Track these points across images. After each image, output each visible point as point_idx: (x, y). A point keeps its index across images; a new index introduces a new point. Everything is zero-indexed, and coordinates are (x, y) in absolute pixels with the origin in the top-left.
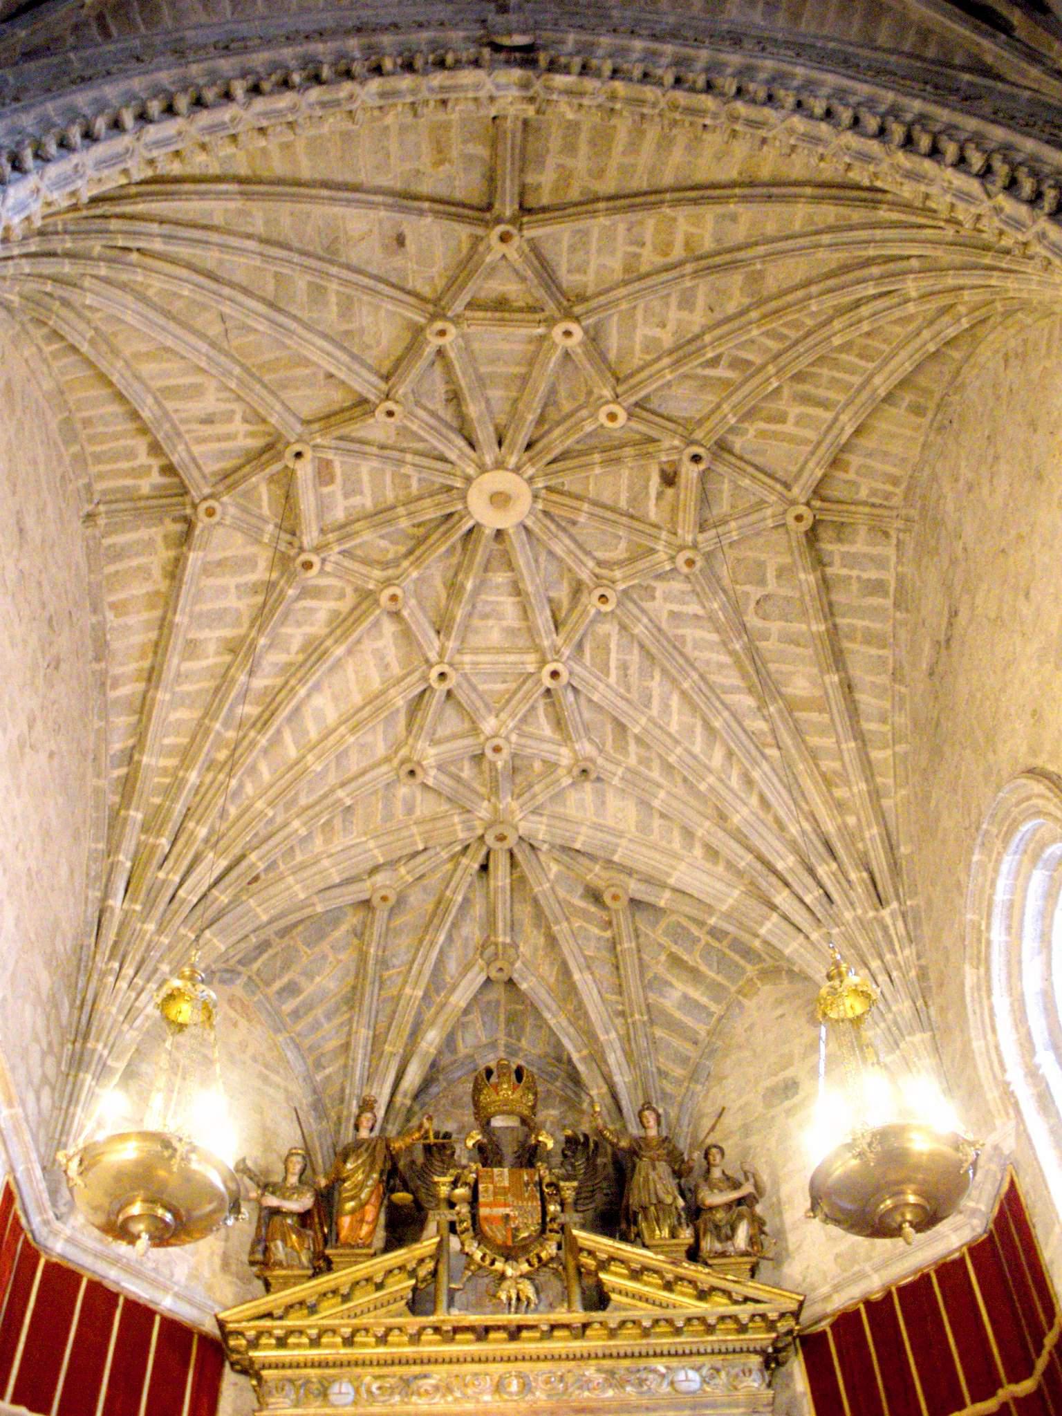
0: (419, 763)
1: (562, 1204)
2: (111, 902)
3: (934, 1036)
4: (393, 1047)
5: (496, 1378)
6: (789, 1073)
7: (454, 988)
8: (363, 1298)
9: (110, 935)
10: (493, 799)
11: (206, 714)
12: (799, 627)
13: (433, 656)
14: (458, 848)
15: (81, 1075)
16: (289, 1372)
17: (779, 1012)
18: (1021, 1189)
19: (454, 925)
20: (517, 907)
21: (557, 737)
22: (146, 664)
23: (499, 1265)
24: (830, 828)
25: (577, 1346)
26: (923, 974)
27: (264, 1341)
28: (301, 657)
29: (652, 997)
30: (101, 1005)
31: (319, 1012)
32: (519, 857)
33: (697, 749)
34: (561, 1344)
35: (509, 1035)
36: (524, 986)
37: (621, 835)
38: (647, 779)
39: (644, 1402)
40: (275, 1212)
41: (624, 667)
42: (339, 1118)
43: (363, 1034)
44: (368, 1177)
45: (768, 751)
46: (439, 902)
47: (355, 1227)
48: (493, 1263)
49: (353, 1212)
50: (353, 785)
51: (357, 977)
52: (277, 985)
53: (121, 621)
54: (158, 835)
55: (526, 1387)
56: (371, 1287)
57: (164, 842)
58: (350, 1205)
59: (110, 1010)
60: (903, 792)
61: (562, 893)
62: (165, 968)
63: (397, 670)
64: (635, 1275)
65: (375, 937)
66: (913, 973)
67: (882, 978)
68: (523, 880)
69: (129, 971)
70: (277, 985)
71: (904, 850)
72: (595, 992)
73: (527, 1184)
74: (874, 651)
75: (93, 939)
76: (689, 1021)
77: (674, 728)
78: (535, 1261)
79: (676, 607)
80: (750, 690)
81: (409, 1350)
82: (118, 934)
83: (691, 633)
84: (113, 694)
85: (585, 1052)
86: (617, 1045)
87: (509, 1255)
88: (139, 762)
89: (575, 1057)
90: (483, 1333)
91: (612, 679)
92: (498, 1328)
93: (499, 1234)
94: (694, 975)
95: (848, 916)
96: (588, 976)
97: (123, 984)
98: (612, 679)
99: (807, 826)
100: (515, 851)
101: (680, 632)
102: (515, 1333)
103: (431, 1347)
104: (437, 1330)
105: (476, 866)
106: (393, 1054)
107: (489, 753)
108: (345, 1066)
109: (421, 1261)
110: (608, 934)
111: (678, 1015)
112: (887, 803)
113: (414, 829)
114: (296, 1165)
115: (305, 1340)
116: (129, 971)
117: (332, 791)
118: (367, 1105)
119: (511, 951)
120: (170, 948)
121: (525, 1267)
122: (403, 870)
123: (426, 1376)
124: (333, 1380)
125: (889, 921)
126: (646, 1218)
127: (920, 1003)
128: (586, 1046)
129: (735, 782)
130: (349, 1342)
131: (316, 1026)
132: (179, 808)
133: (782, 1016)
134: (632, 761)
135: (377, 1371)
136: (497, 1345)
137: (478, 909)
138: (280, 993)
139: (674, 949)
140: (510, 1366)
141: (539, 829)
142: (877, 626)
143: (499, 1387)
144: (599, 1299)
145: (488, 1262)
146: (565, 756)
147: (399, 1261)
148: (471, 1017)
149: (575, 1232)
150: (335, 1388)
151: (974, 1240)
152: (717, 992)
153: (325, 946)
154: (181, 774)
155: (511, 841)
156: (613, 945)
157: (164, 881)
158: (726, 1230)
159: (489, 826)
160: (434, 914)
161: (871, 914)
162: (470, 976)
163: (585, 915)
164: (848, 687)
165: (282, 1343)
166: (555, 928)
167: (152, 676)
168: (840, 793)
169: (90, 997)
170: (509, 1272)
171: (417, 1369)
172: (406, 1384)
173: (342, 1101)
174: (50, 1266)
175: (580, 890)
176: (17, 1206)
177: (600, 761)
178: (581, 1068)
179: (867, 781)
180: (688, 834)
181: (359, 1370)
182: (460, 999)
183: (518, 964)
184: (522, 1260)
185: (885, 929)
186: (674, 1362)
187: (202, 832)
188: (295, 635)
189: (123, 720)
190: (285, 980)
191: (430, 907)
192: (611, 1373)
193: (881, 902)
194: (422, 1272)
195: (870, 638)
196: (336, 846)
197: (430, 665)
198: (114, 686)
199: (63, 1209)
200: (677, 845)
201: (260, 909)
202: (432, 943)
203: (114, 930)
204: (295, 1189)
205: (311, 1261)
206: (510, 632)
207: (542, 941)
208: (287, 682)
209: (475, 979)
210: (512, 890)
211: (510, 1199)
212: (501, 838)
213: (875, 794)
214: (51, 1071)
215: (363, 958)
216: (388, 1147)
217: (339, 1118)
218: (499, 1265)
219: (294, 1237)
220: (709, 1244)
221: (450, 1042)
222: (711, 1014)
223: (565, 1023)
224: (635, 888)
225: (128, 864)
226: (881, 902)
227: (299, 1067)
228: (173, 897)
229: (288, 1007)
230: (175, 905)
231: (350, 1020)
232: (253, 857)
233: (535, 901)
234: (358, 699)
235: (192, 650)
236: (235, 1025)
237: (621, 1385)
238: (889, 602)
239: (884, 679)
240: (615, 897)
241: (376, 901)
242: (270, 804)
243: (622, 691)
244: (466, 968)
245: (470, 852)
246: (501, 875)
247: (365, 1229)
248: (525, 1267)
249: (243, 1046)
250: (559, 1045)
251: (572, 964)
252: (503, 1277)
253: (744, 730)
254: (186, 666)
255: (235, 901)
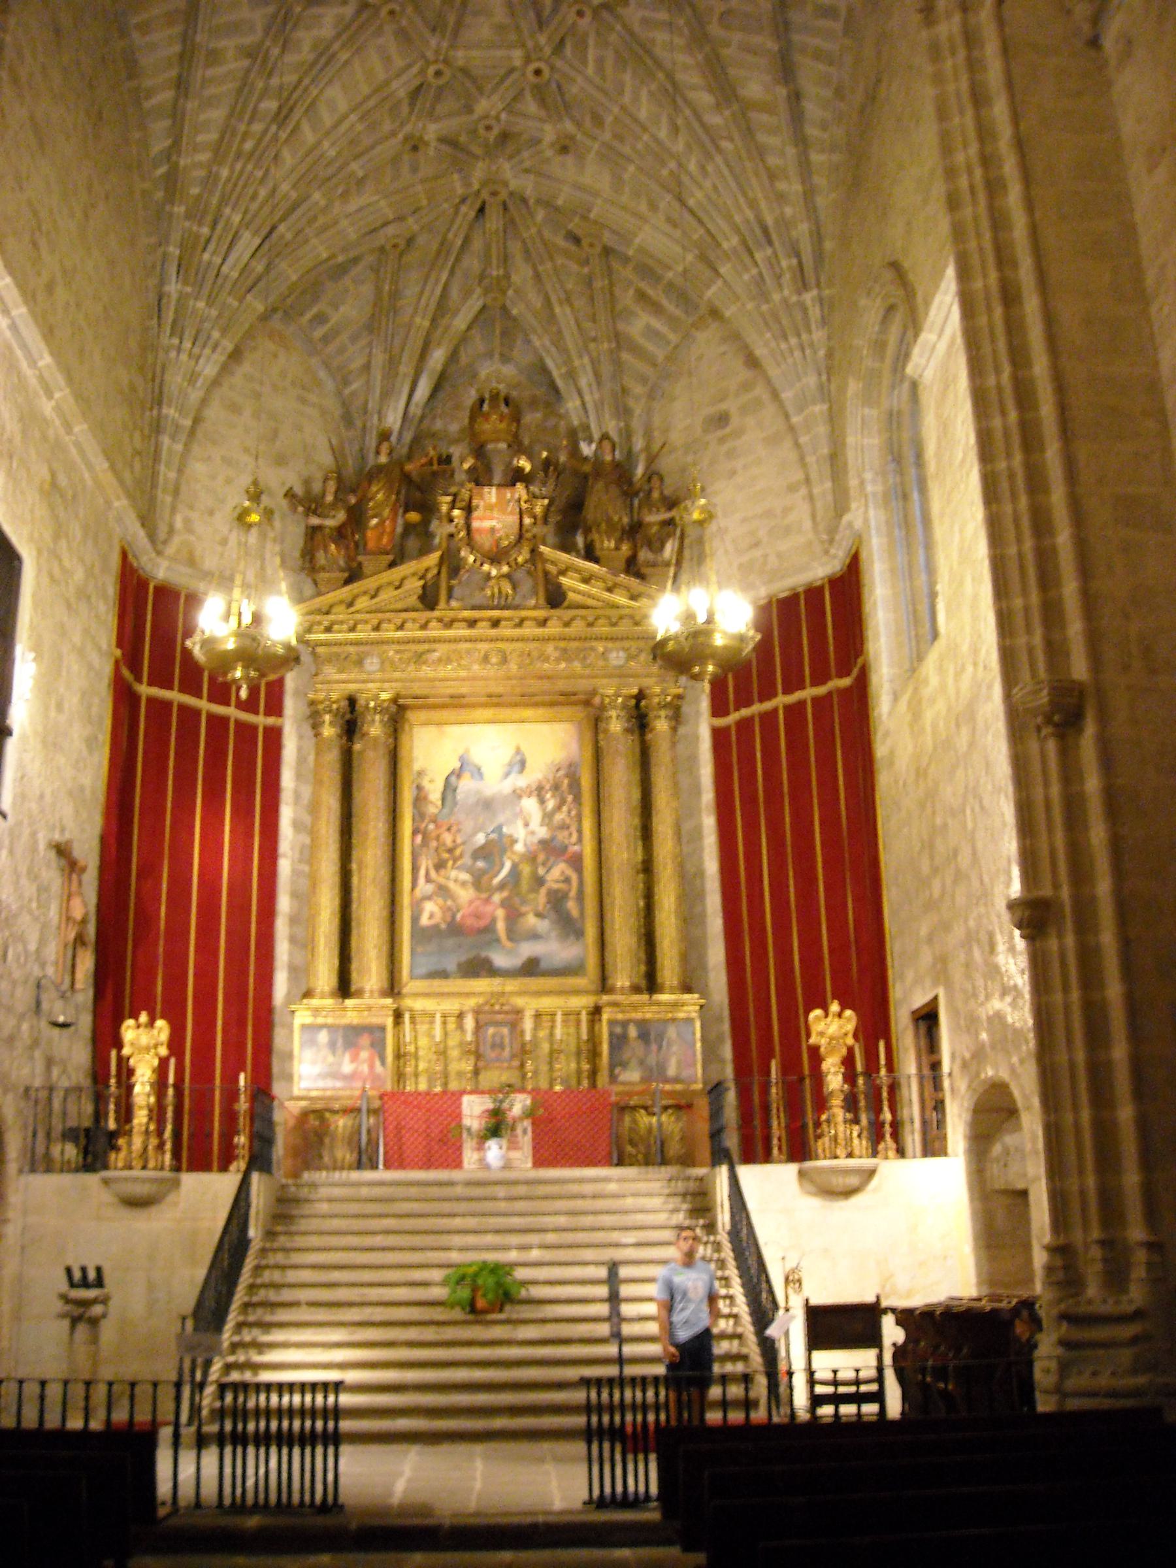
0: (421, 138)
1: (535, 517)
2: (167, 288)
3: (830, 408)
4: (406, 368)
5: (483, 653)
6: (723, 406)
7: (458, 311)
8: (386, 595)
9: (170, 315)
10: (487, 161)
11: (231, 115)
12: (756, 40)
13: (430, 55)
14: (457, 200)
15: (161, 438)
16: (335, 649)
17: (723, 348)
18: (864, 555)
19: (458, 260)
20: (509, 243)
21: (543, 113)
22: (174, 73)
23: (486, 567)
24: (769, 220)
25: (539, 631)
26: (830, 355)
27: (315, 628)
28: (311, 57)
29: (621, 326)
30: (167, 377)
31: (344, 337)
32: (511, 207)
33: (663, 134)
34: (529, 630)
35: (502, 345)
36: (515, 312)
37: (596, 194)
38: (620, 154)
39: (587, 672)
40: (318, 528)
41: (600, 61)
42: (364, 427)
43: (379, 358)
44: (387, 498)
45: (725, 144)
46: (442, 244)
47: (380, 538)
48: (482, 565)
49: (376, 526)
50: (365, 158)
51: (375, 305)
52: (309, 315)
53: (147, 39)
54: (200, 224)
55: (504, 660)
56: (391, 588)
57: (205, 231)
58: (374, 521)
59: (175, 380)
60: (834, 195)
61: (547, 234)
62: (216, 334)
63: (399, 63)
64: (586, 581)
65: (389, 276)
66: (822, 353)
67: (797, 354)
68: (512, 222)
69: (187, 345)
70: (309, 315)
71: (828, 245)
72: (572, 322)
73: (509, 501)
74: (821, 67)
75: (155, 321)
76: (650, 347)
77: (643, 114)
78: (513, 564)
79: (648, 14)
80: (710, 90)
81: (420, 634)
82: (176, 312)
83: (661, 37)
84: (147, 105)
85: (564, 370)
86: (589, 368)
87: (495, 560)
88: (177, 163)
89: (556, 374)
90: (472, 623)
91: (590, 70)
92: (482, 620)
93: (485, 541)
94: (657, 309)
95: (776, 297)
96: (568, 310)
97: (184, 357)
98: (590, 70)
99: (750, 215)
100: (508, 201)
101: (651, 35)
102: (496, 623)
103: (435, 631)
104: (440, 620)
105: (472, 214)
106: (405, 375)
107: (482, 131)
108: (368, 382)
109: (427, 570)
110: (586, 270)
111: (642, 341)
112: (820, 201)
113: (419, 188)
114: (332, 486)
115: (345, 627)
116: (187, 345)
117: (346, 164)
118: (385, 436)
119: (504, 283)
120: (219, 316)
121: (505, 569)
122: (410, 220)
123: (434, 651)
124: (367, 654)
125: (809, 303)
126: (599, 532)
127: (824, 378)
128: (565, 363)
129: (692, 167)
130: (377, 628)
131: (342, 350)
132: (215, 201)
133: (724, 353)
134: (607, 136)
135: (397, 647)
136: (483, 629)
137: (477, 244)
138: (311, 321)
139: (643, 285)
140: (492, 645)
141: (527, 185)
142: (826, 45)
143: (486, 659)
144: (555, 598)
145: (478, 563)
146: (549, 133)
147: (412, 570)
148: (473, 331)
149: (542, 548)
150: (368, 661)
151: (833, 574)
152: (673, 321)
153: (347, 281)
154: (215, 169)
155: (504, 195)
156: (589, 281)
157: (209, 263)
158: (657, 545)
159: (484, 184)
160: (439, 253)
161: (794, 299)
162: (469, 302)
163: (567, 254)
164: (796, 97)
165: (328, 630)
166: (541, 268)
167: (181, 85)
168: (781, 186)
169: (158, 369)
170: (494, 572)
171: (426, 646)
172: (419, 658)
173: (366, 412)
174: (156, 588)
175: (563, 232)
176: (130, 556)
177: (579, 137)
178: (560, 383)
179: (803, 182)
180: (653, 207)
181: (385, 647)
182: (460, 322)
183: (510, 292)
184: (504, 563)
185: (805, 310)
186: (610, 645)
187: (237, 219)
188: (306, 39)
189: (160, 126)
190: (315, 310)
191: (435, 246)
192: (565, 650)
193: (803, 285)
194: (430, 575)
195: (818, 55)
196: (352, 207)
197: (428, 63)
198: (148, 97)
199: (160, 547)
200: (643, 207)
201: (290, 272)
202: (437, 281)
203: (172, 308)
204: (333, 505)
205: (346, 563)
206: (500, 28)
207: (530, 273)
208: (300, 81)
209: (474, 304)
210: (505, 232)
211: (496, 514)
212: (494, 194)
213: (809, 194)
214: (138, 444)
215: (378, 290)
216: (402, 469)
217: (364, 427)
218: (486, 567)
219: (333, 547)
220: (644, 555)
221: (453, 357)
222: (668, 343)
223: (548, 343)
224: (607, 238)
225: (177, 252)
226: (805, 286)
227: (330, 385)
228: (217, 275)
229: (318, 333)
230: (220, 281)
231: (370, 344)
232: (282, 228)
233: (524, 242)
234: (365, 89)
235: (214, 57)
236: (275, 356)
237: (569, 660)
238: (838, 26)
239: (828, 93)
240: (591, 245)
241: (388, 247)
242: (294, 186)
243: (597, 80)
244: (467, 294)
245: (469, 202)
246: (494, 221)
247: (385, 540)
248: (505, 569)
249: (283, 374)
250: (541, 360)
251: (554, 299)
252: (488, 577)
253: (703, 125)
254: (210, 72)
255: (269, 268)
